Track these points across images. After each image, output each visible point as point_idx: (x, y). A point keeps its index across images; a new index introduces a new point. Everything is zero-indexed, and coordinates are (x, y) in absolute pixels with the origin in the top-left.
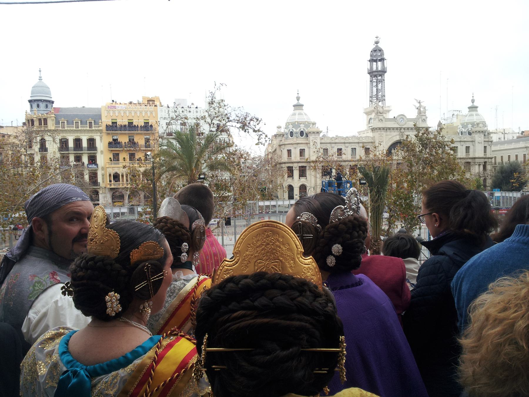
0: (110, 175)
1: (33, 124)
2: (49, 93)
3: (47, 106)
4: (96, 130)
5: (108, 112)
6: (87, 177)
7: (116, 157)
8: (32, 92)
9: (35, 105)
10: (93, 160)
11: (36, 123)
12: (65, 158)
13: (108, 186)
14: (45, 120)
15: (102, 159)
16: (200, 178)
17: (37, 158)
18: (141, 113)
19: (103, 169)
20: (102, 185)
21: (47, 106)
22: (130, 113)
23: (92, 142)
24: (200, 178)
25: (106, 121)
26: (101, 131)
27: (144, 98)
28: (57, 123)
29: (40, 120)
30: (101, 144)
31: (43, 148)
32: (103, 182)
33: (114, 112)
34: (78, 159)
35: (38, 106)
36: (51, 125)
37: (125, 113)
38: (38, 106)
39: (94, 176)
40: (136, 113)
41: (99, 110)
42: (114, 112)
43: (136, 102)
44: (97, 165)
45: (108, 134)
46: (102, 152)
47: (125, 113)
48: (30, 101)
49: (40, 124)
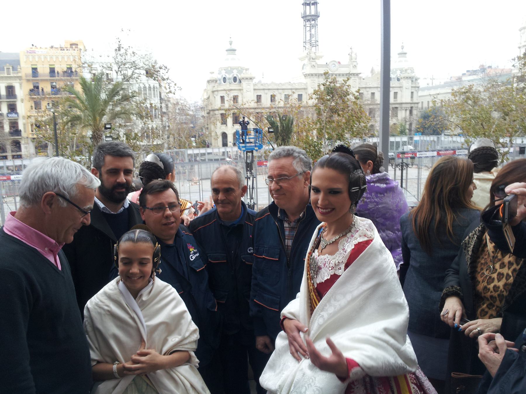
0: (32, 125)
4: (15, 77)
5: (27, 57)
7: (37, 106)
10: (12, 108)
13: (31, 136)
15: (23, 108)
16: (106, 128)
18: (63, 58)
19: (24, 117)
20: (23, 134)
22: (51, 58)
24: (106, 128)
26: (20, 78)
30: (22, 92)
32: (25, 131)
33: (33, 57)
37: (45, 58)
39: (14, 125)
40: (57, 58)
41: (18, 55)
42: (33, 57)
44: (17, 113)
47: (45, 58)
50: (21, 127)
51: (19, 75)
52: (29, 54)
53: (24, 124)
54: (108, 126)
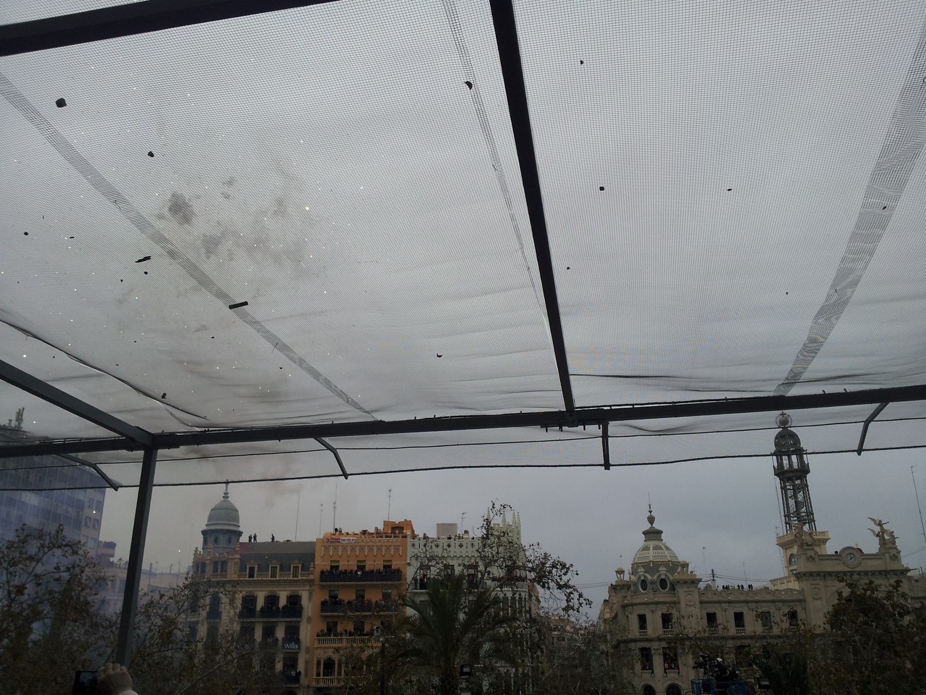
0: (319, 663)
1: (203, 571)
2: (236, 519)
3: (230, 541)
5: (327, 549)
6: (279, 666)
8: (210, 518)
9: (211, 539)
10: (293, 634)
11: (209, 569)
12: (247, 630)
13: (314, 684)
14: (224, 563)
15: (307, 633)
16: (462, 673)
17: (202, 631)
18: (379, 549)
19: (308, 650)
20: (304, 681)
21: (230, 541)
22: (362, 549)
23: (294, 600)
24: (462, 673)
25: (321, 563)
26: (311, 582)
27: (386, 523)
28: (242, 569)
29: (216, 563)
30: (310, 605)
31: (214, 613)
32: (306, 675)
33: (336, 549)
34: (269, 632)
35: (216, 540)
36: (232, 574)
37: (353, 549)
38: (216, 540)
39: (291, 662)
40: (371, 549)
42: (336, 549)
43: (372, 530)
45: (322, 587)
46: (309, 620)
47: (353, 549)
48: (204, 532)
49: (215, 570)
50: (301, 667)
51: (311, 577)
52: (329, 544)
53: (307, 663)
54: (466, 670)
